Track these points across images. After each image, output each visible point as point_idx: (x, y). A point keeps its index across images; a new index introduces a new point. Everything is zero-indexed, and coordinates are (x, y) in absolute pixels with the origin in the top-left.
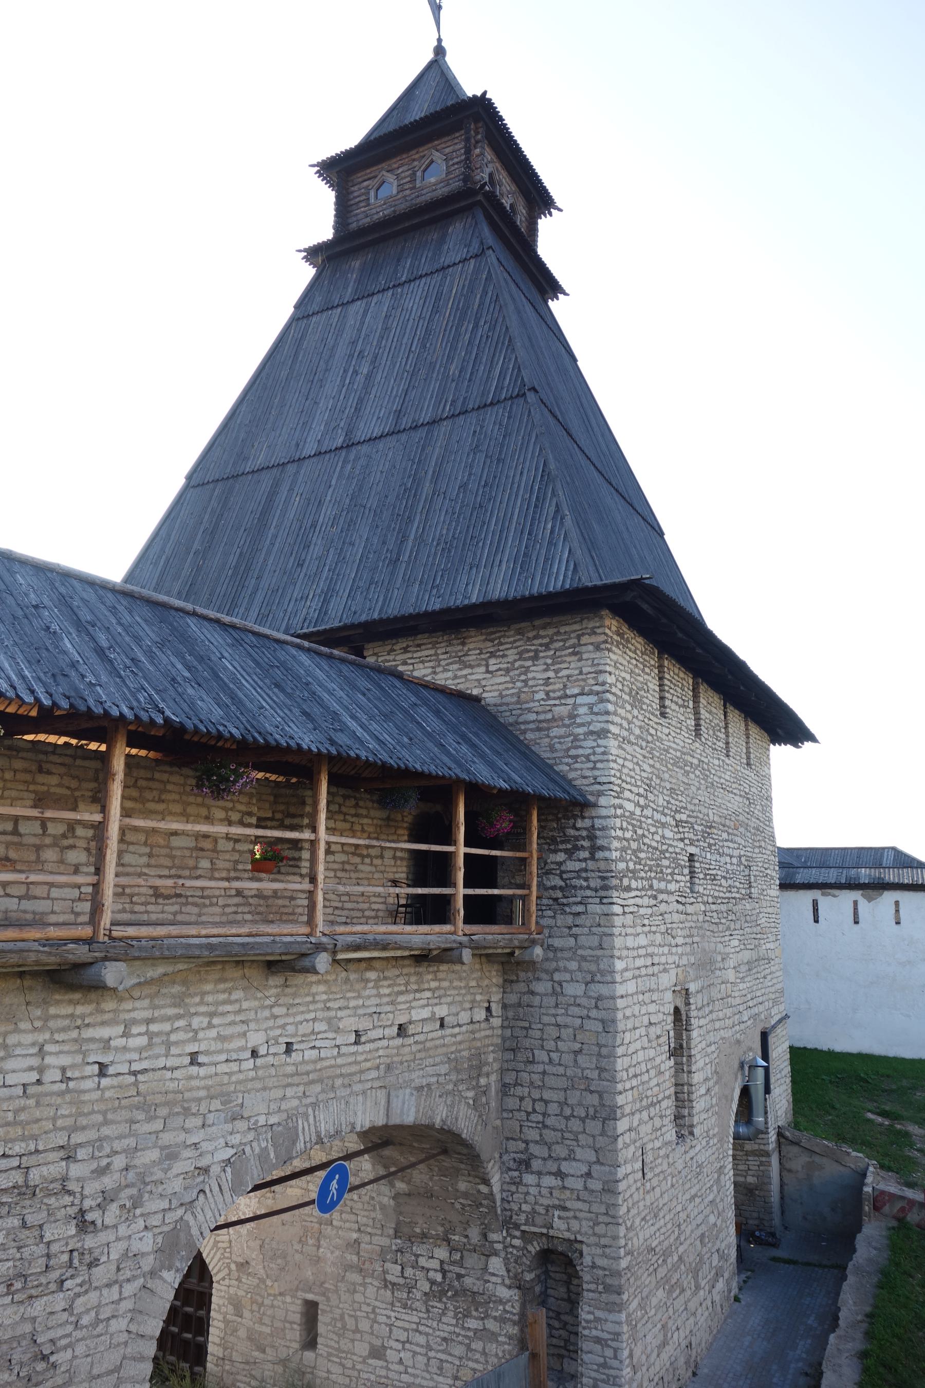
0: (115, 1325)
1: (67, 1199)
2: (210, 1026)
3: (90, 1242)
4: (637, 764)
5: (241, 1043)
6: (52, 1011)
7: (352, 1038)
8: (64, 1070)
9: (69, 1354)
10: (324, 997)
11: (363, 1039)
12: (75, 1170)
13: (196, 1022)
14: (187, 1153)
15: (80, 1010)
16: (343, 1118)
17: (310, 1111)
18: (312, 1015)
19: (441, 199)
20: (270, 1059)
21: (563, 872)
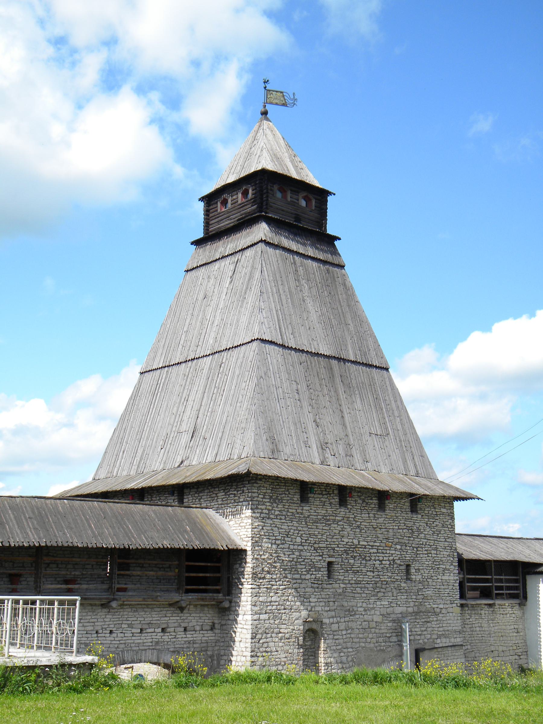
4: (276, 527)
5: (91, 628)
7: (139, 631)
10: (126, 616)
11: (144, 632)
16: (135, 657)
17: (120, 653)
18: (121, 622)
20: (103, 635)
21: (238, 572)
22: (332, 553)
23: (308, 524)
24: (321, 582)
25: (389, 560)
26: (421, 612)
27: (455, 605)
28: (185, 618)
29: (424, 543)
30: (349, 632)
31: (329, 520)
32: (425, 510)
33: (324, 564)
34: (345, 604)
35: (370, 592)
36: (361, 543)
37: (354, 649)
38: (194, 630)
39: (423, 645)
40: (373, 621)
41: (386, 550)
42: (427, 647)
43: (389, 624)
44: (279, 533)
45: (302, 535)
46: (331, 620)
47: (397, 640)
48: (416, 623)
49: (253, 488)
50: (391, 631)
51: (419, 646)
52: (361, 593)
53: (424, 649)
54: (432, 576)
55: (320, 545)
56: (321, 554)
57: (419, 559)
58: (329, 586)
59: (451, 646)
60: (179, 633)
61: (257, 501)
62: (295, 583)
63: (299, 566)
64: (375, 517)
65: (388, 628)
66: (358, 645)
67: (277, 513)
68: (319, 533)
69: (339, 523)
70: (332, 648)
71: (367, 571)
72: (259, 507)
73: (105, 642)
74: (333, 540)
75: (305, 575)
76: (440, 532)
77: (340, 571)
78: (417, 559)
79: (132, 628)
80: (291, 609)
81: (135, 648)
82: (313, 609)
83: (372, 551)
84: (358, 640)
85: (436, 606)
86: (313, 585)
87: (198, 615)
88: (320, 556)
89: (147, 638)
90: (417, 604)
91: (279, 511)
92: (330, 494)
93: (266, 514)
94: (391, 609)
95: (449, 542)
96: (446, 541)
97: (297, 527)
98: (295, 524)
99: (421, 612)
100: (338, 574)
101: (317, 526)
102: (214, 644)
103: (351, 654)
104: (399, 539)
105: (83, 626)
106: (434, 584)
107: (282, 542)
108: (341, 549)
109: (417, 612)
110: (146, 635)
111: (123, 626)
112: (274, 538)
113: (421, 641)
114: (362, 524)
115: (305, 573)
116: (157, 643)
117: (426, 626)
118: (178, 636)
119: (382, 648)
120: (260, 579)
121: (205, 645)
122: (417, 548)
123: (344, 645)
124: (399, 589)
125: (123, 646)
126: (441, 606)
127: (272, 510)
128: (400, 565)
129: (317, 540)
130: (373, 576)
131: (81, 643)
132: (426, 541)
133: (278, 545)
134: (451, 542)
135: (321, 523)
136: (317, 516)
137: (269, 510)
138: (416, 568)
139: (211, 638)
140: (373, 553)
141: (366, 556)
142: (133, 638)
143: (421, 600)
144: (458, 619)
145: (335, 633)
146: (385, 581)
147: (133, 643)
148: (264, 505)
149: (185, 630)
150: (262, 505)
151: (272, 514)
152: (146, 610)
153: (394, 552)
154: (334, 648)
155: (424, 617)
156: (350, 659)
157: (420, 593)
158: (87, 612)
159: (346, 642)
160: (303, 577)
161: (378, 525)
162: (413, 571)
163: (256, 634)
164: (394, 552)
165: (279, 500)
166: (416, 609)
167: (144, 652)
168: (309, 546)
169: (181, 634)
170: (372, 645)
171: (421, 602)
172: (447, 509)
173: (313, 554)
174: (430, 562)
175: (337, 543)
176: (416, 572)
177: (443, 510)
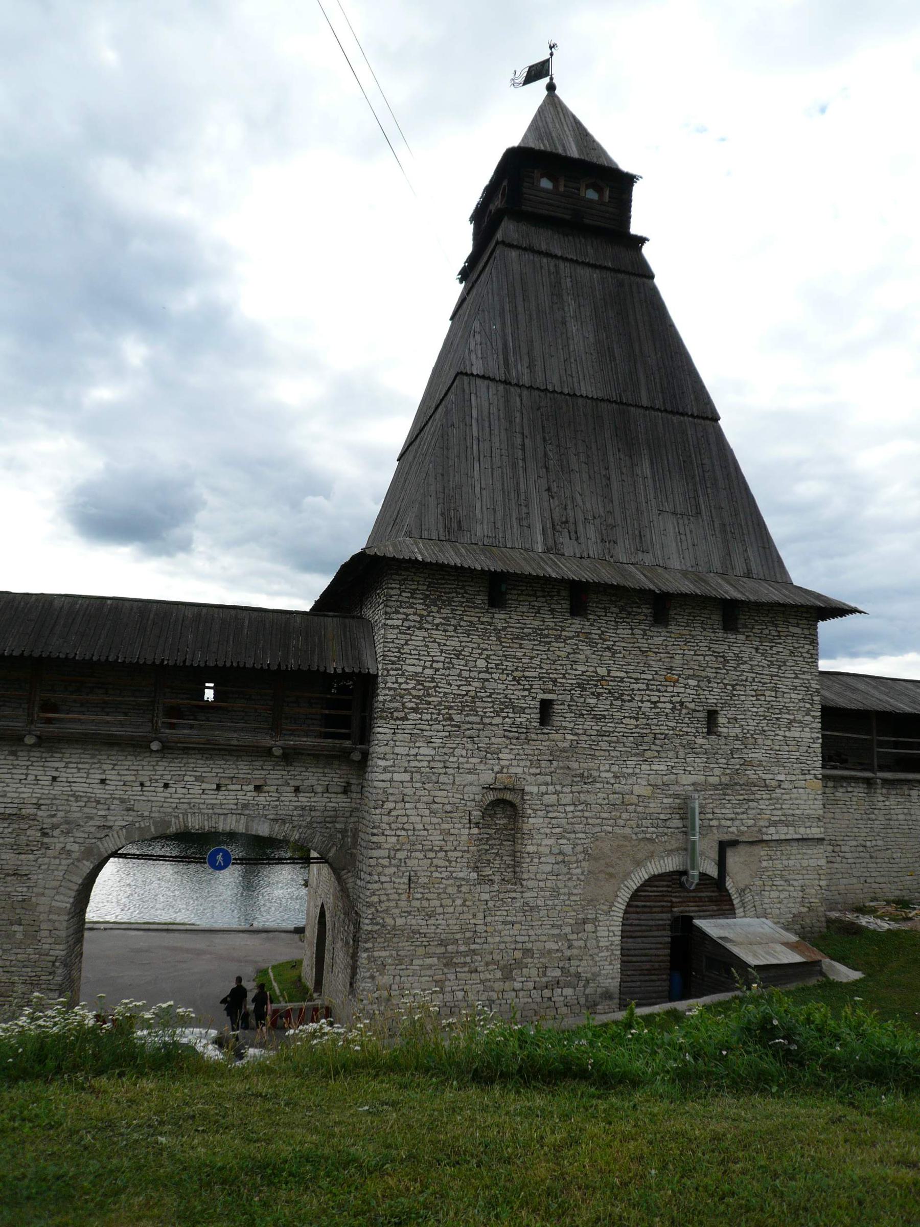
0: (56, 873)
1: (36, 823)
2: (113, 769)
3: (46, 840)
4: (434, 642)
5: (133, 778)
6: (32, 754)
7: (215, 787)
8: (36, 776)
9: (35, 877)
11: (224, 789)
12: (40, 813)
13: (105, 767)
14: (97, 818)
15: (44, 755)
16: (206, 823)
17: (181, 815)
19: (557, 211)
22: (551, 687)
23: (503, 640)
24: (525, 731)
25: (671, 702)
26: (736, 784)
27: (811, 777)
28: (296, 773)
29: (750, 679)
30: (580, 808)
31: (547, 636)
32: (753, 628)
33: (533, 703)
34: (575, 765)
35: (629, 750)
36: (613, 674)
37: (589, 835)
38: (313, 792)
39: (737, 836)
40: (632, 793)
41: (667, 686)
43: (665, 801)
44: (442, 651)
45: (488, 657)
46: (543, 789)
47: (681, 825)
48: (724, 801)
49: (392, 581)
50: (669, 811)
51: (726, 837)
52: (609, 751)
53: (734, 843)
54: (764, 731)
55: (526, 674)
56: (527, 687)
57: (736, 702)
58: (541, 737)
59: (798, 840)
60: (285, 794)
61: (397, 601)
62: (469, 729)
63: (478, 704)
64: (645, 634)
65: (663, 806)
66: (598, 829)
67: (437, 621)
68: (524, 655)
69: (568, 642)
70: (542, 831)
71: (625, 717)
72: (401, 610)
73: (156, 799)
74: (554, 667)
75: (493, 717)
76: (785, 662)
77: (566, 715)
78: (732, 702)
79: (203, 782)
80: (458, 768)
81: (206, 811)
82: (505, 770)
83: (636, 686)
84: (599, 821)
85: (771, 776)
86: (506, 733)
87: (321, 771)
88: (524, 690)
89: (228, 797)
90: (728, 771)
91: (444, 618)
92: (552, 597)
93: (415, 621)
94: (673, 777)
95: (803, 679)
96: (797, 678)
97: (479, 644)
98: (476, 639)
99: (736, 784)
100: (562, 719)
101: (521, 644)
102: (348, 814)
103: (583, 841)
104: (694, 669)
105: (118, 774)
106: (769, 742)
107: (446, 665)
108: (569, 681)
109: (727, 785)
110: (226, 793)
111: (186, 778)
112: (430, 659)
113: (733, 829)
114: (617, 644)
115: (492, 715)
116: (245, 806)
117: (746, 806)
118: (282, 798)
119: (648, 836)
120: (397, 719)
121: (332, 813)
122: (733, 686)
124: (691, 746)
125: (185, 806)
126: (782, 777)
127: (428, 616)
128: (695, 711)
129: (521, 665)
130: (637, 726)
131: (114, 798)
132: (754, 675)
133: (437, 670)
134: (808, 680)
135: (530, 640)
136: (523, 629)
137: (421, 616)
138: (729, 716)
139: (344, 805)
140: (639, 690)
141: (622, 695)
142: (203, 796)
143: (738, 767)
144: (816, 799)
145: (550, 809)
146: (662, 734)
147: (204, 803)
148: (412, 607)
149: (297, 790)
150: (407, 608)
151: (428, 622)
152: (228, 758)
153: (682, 690)
155: (742, 792)
156: (579, 849)
157: (735, 756)
158: (126, 756)
159: (572, 824)
160: (487, 721)
161: (651, 646)
162: (722, 720)
163: (384, 802)
164: (682, 690)
165: (443, 601)
166: (726, 780)
167: (222, 817)
168: (502, 673)
169: (288, 797)
170: (627, 831)
171: (737, 770)
172: (803, 629)
173: (509, 687)
174: (762, 709)
175: (563, 672)
176: (729, 722)
177: (792, 629)
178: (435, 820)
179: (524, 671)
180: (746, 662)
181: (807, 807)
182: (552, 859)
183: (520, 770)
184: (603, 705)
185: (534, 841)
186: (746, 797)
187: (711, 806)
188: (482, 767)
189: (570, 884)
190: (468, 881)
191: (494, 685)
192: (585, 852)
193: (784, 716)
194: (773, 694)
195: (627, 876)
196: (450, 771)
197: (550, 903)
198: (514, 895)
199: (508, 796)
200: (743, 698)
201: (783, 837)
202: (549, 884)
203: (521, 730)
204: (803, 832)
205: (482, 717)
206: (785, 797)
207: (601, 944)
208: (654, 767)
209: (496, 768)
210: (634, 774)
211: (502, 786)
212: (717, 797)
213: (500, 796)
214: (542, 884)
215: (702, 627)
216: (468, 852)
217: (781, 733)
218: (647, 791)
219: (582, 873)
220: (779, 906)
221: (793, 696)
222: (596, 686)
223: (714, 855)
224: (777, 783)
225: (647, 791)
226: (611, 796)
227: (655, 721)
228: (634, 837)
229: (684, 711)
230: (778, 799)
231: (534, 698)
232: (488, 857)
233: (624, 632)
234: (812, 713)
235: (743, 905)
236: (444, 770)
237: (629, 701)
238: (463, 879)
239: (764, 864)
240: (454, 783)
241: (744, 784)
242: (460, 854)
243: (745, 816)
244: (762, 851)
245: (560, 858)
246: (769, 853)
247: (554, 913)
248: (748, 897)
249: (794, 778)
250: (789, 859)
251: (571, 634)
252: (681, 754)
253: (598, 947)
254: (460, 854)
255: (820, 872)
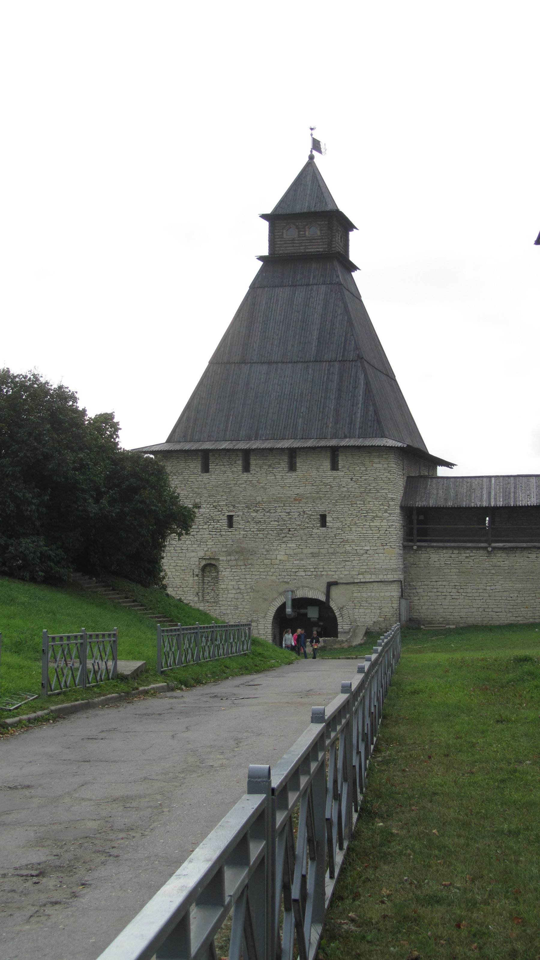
26: (338, 553)
30: (248, 567)
37: (254, 580)
42: (339, 581)
43: (295, 562)
47: (304, 575)
53: (336, 583)
54: (356, 523)
55: (219, 503)
66: (258, 577)
70: (229, 578)
71: (271, 521)
82: (209, 550)
84: (259, 573)
86: (210, 533)
90: (333, 546)
91: (179, 481)
95: (382, 493)
99: (338, 553)
113: (336, 576)
119: (285, 580)
122: (336, 500)
123: (243, 576)
126: (368, 548)
130: (278, 525)
132: (350, 493)
134: (386, 493)
136: (218, 482)
141: (270, 510)
144: (391, 559)
154: (232, 578)
156: (248, 586)
159: (245, 575)
160: (201, 527)
162: (328, 519)
170: (274, 577)
171: (339, 545)
172: (383, 465)
178: (177, 574)
179: (218, 502)
180: (344, 487)
181: (385, 564)
182: (234, 592)
183: (216, 550)
184: (259, 516)
185: (225, 583)
186: (344, 559)
187: (322, 564)
188: (198, 549)
189: (243, 603)
190: (193, 601)
191: (204, 510)
192: (251, 588)
193: (369, 514)
194: (362, 503)
195: (274, 599)
196: (184, 551)
197: (234, 612)
198: (215, 608)
199: (213, 562)
200: (343, 506)
201: (367, 580)
202: (233, 603)
203: (217, 531)
204: (381, 577)
205: (198, 525)
206: (369, 558)
207: (260, 632)
208: (288, 545)
209: (206, 549)
210: (277, 549)
211: (208, 558)
212: (326, 560)
213: (208, 562)
214: (229, 603)
215: (317, 471)
216: (193, 588)
217: (368, 524)
218: (285, 558)
219: (250, 598)
220: (364, 617)
221: (375, 503)
222: (256, 506)
223: (325, 590)
224: (364, 552)
225: (285, 558)
226: (265, 561)
227: (289, 522)
228: (278, 581)
229: (305, 516)
230: (364, 560)
231: (223, 515)
232: (208, 591)
233: (271, 478)
234: (389, 512)
235: (342, 616)
236: (181, 551)
237: (274, 513)
238: (191, 600)
239: (355, 595)
240: (185, 557)
241: (342, 553)
242: (189, 589)
243: (343, 569)
244: (355, 588)
245: (238, 591)
246: (358, 589)
247: (235, 617)
248: (345, 612)
249: (376, 548)
250: (371, 592)
251: (242, 482)
252: (304, 538)
253: (259, 634)
254: (189, 589)
255: (392, 599)
